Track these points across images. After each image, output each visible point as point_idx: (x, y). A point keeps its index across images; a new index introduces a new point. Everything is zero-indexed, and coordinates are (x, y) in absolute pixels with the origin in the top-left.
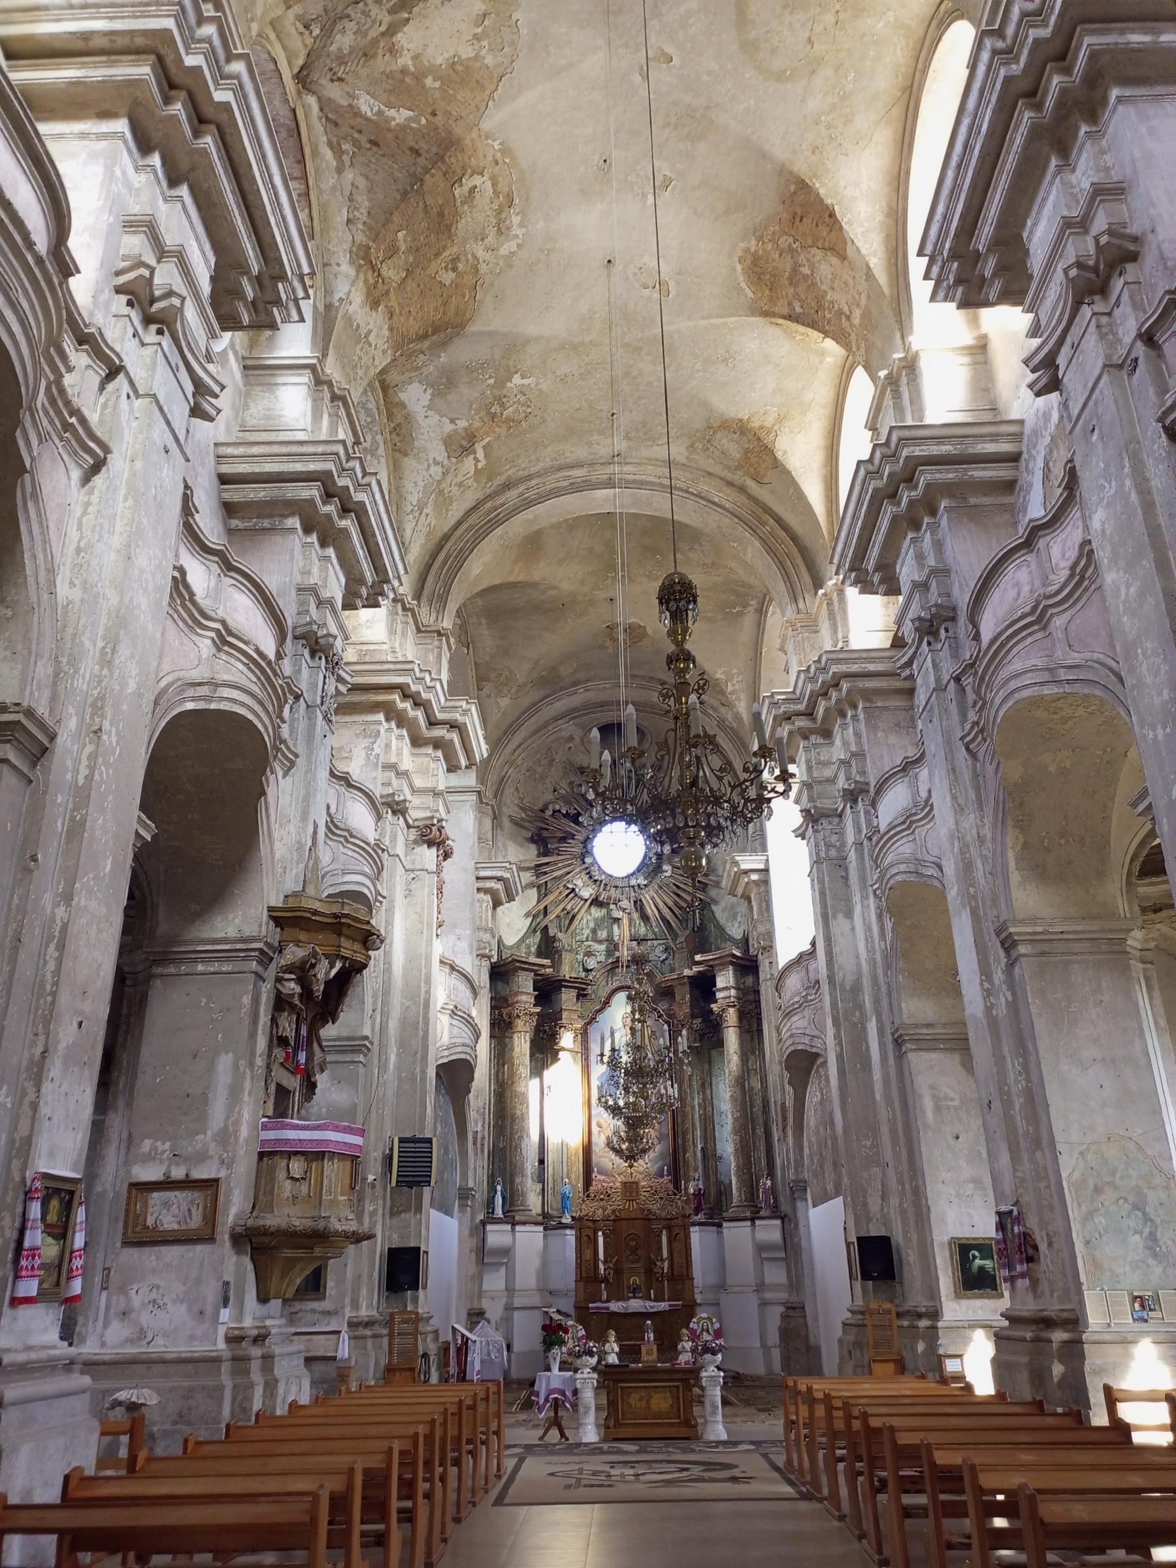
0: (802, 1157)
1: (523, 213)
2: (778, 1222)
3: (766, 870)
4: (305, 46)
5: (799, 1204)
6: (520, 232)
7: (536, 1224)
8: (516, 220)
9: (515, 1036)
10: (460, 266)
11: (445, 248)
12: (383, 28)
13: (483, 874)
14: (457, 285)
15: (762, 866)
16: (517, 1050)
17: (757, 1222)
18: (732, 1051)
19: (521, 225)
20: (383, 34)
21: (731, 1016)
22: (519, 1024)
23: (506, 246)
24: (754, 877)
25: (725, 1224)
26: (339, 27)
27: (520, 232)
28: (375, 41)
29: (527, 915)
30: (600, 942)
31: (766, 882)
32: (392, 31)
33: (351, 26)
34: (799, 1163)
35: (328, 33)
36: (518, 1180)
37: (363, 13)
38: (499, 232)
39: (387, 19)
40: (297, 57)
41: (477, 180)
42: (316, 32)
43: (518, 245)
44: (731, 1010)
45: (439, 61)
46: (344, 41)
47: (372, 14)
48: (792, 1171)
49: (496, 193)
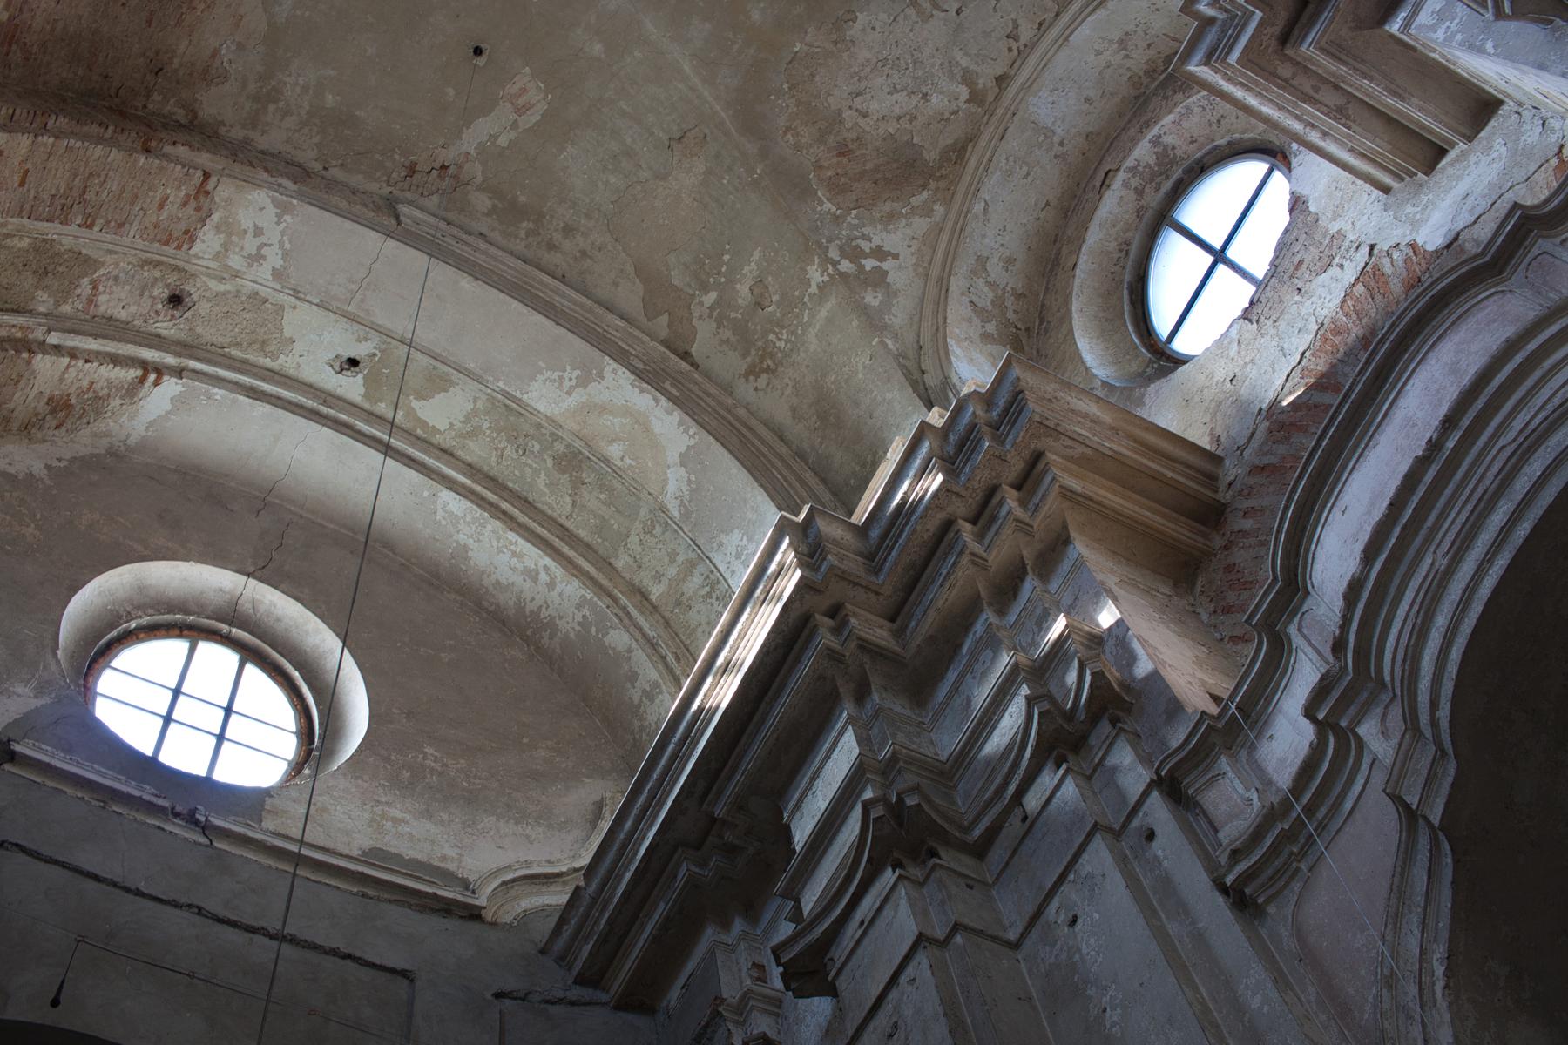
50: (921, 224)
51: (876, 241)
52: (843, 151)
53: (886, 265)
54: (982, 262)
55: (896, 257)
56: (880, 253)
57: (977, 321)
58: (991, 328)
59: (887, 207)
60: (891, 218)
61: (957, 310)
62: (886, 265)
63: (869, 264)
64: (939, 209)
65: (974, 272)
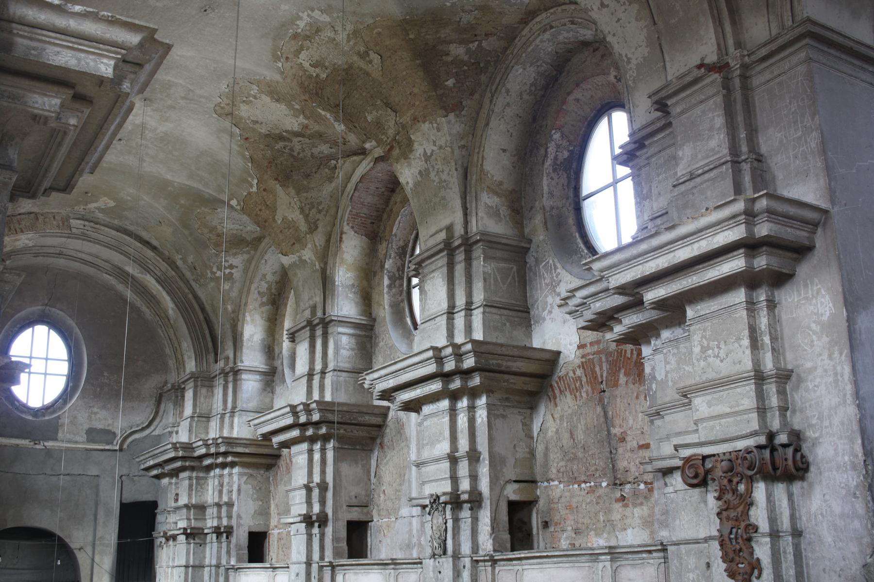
1: (292, 22)
4: (345, 162)
6: (304, 16)
8: (301, 24)
10: (362, 49)
11: (361, 69)
12: (301, 139)
14: (376, 45)
19: (301, 19)
20: (303, 136)
23: (322, 19)
26: (321, 155)
27: (304, 16)
28: (311, 137)
32: (297, 134)
33: (315, 151)
35: (330, 157)
37: (304, 151)
38: (318, 30)
39: (296, 140)
40: (354, 161)
41: (306, 65)
42: (333, 162)
43: (313, 10)
45: (284, 107)
46: (324, 149)
47: (300, 147)
49: (302, 48)
50: (246, 256)
51: (230, 262)
52: (218, 235)
53: (233, 271)
54: (264, 276)
55: (237, 267)
56: (231, 267)
57: (259, 299)
58: (265, 299)
59: (235, 251)
60: (235, 254)
61: (254, 295)
62: (233, 271)
63: (227, 271)
64: (252, 252)
65: (261, 280)
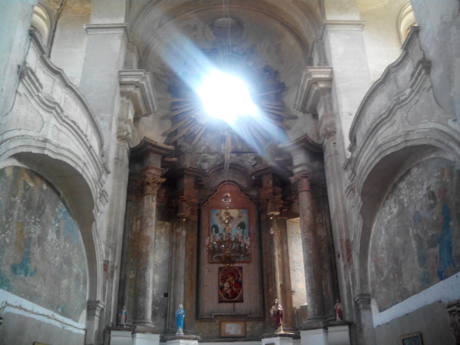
0: (366, 277)
2: (347, 327)
3: (330, 80)
5: (364, 313)
7: (154, 332)
9: (145, 198)
13: (124, 80)
15: (327, 76)
16: (146, 206)
17: (330, 329)
18: (305, 207)
21: (305, 184)
22: (149, 188)
24: (322, 85)
25: (303, 334)
29: (163, 135)
30: (212, 154)
31: (329, 90)
34: (364, 281)
36: (141, 300)
44: (305, 180)
48: (358, 288)
